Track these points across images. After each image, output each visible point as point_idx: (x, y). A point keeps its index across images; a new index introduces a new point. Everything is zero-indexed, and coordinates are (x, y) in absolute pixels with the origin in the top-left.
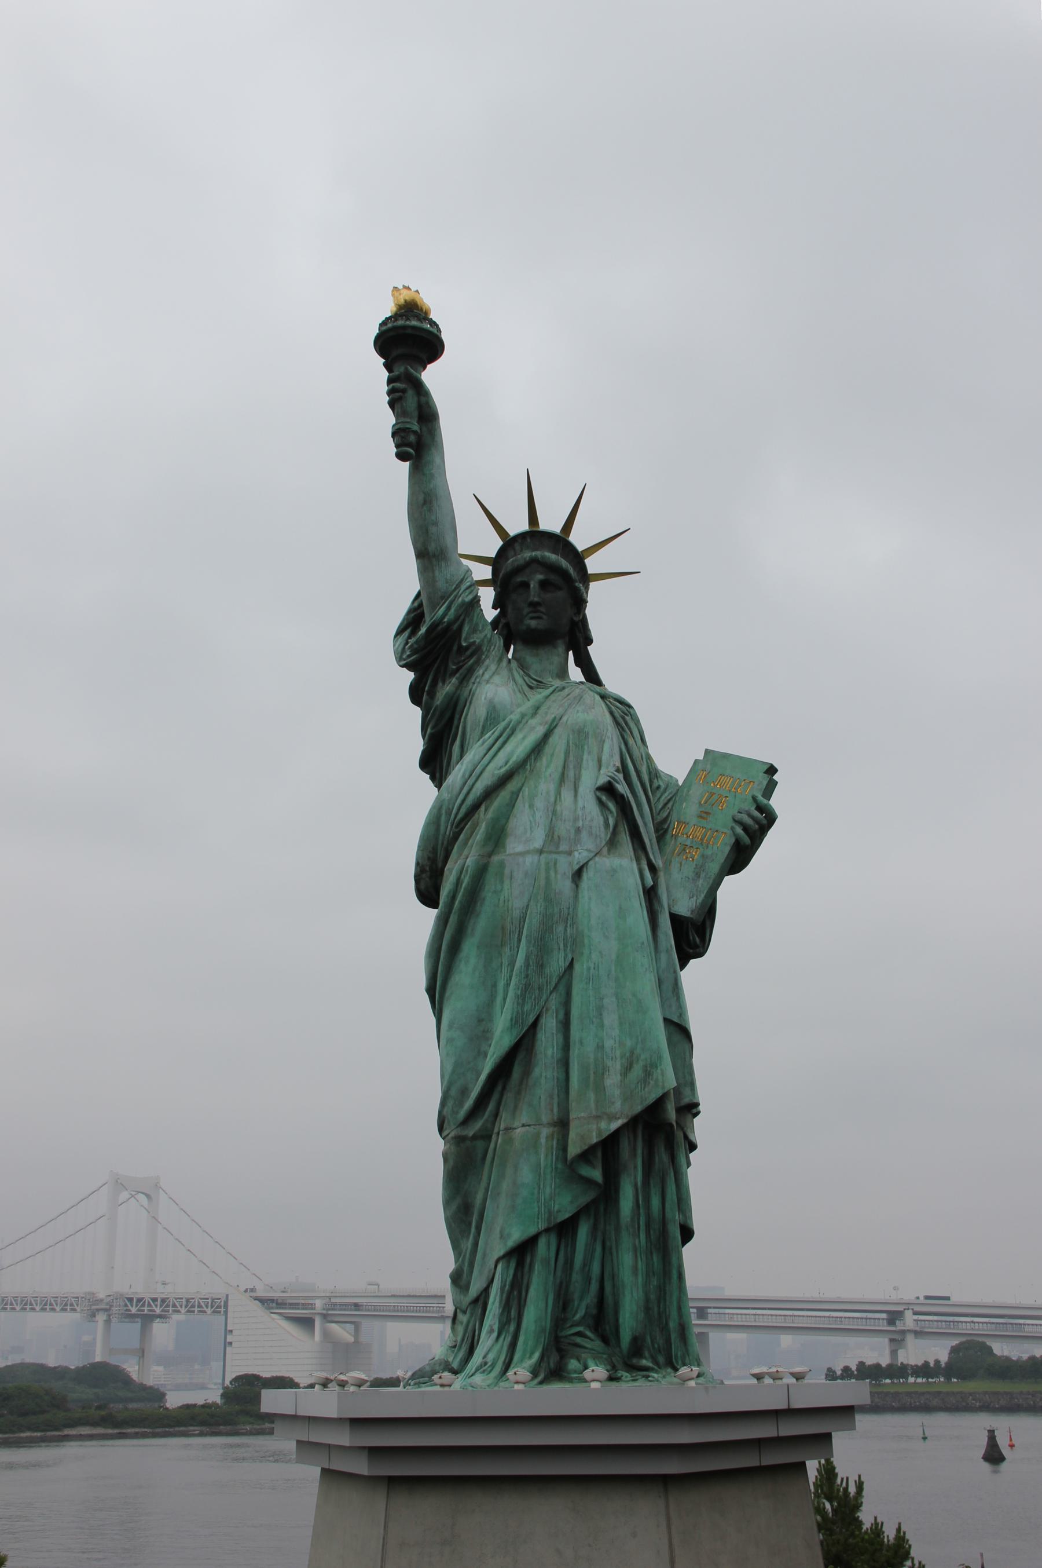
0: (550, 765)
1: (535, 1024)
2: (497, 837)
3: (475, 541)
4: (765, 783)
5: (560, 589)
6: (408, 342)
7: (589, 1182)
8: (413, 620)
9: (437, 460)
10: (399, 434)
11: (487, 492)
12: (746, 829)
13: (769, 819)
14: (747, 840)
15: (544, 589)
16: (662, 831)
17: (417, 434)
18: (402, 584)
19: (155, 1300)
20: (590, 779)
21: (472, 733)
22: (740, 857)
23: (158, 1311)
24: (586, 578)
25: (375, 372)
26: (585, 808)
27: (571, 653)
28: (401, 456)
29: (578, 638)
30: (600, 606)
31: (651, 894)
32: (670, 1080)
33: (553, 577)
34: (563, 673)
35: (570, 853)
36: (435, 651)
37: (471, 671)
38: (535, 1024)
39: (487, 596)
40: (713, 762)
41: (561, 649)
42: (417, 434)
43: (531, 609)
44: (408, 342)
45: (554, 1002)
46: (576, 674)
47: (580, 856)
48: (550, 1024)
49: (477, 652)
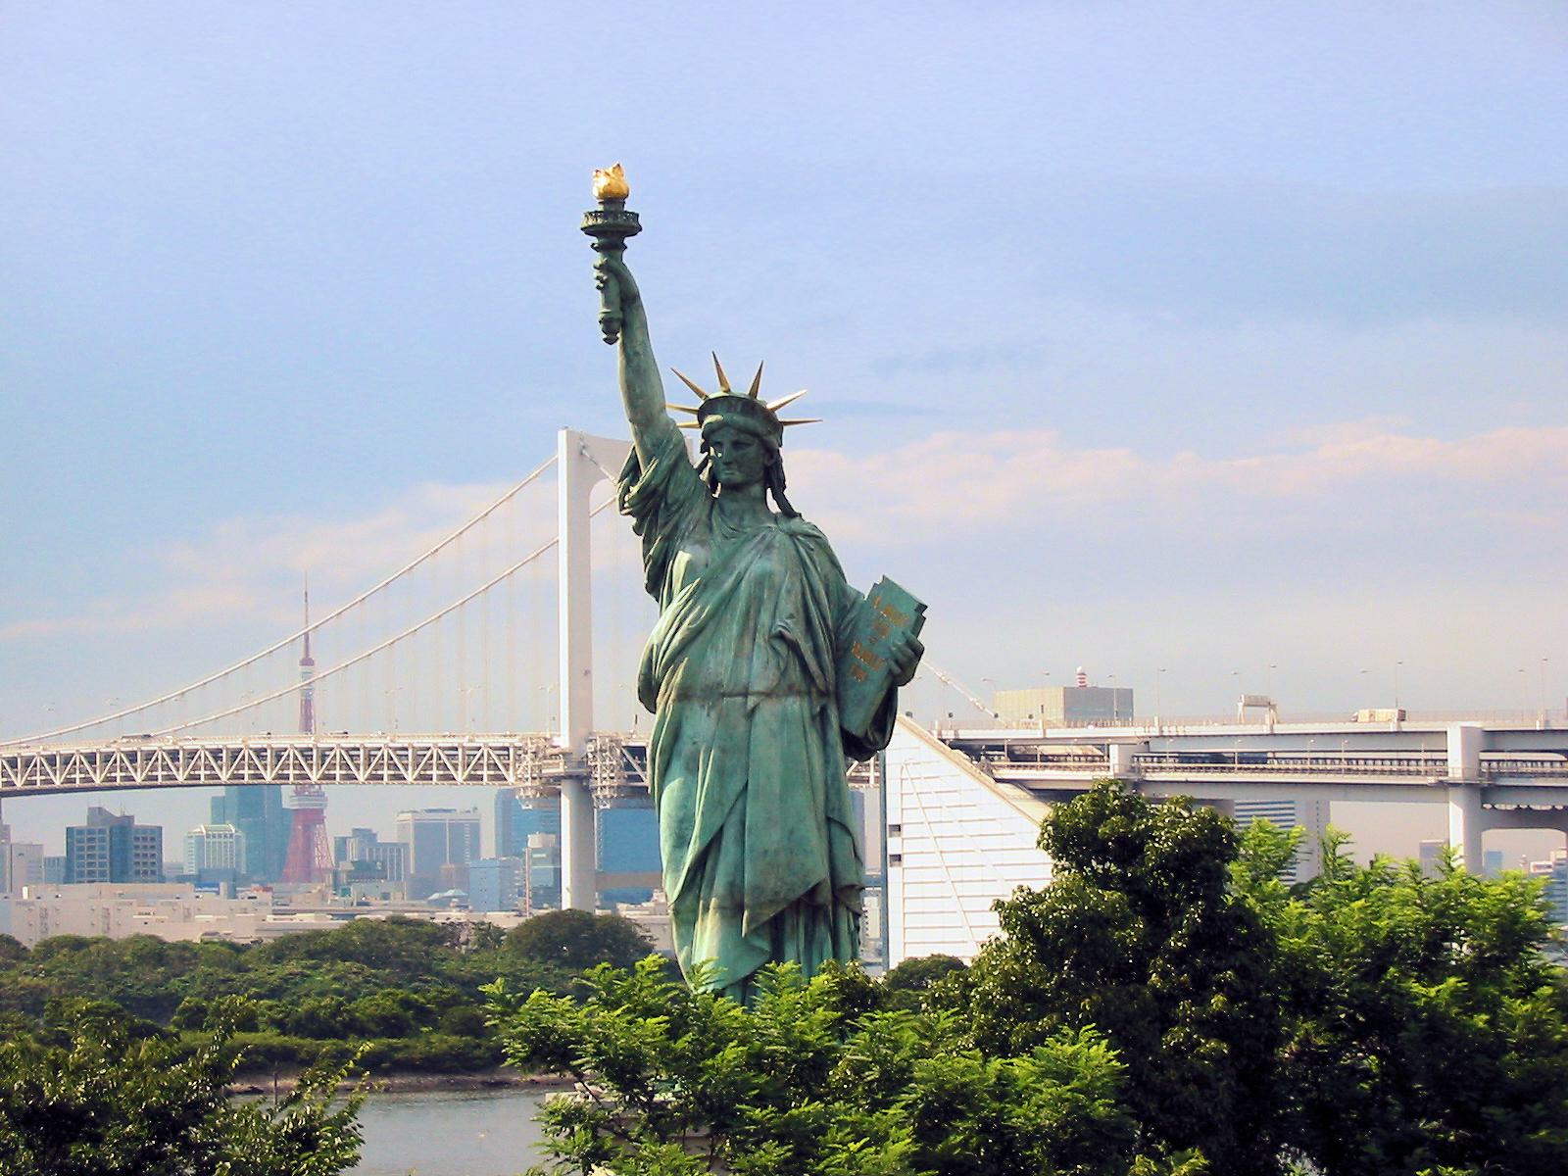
1: (721, 829)
4: (914, 618)
5: (749, 445)
6: (613, 226)
7: (762, 950)
9: (639, 337)
12: (897, 662)
13: (918, 652)
14: (897, 670)
17: (623, 312)
21: (677, 586)
24: (778, 427)
27: (769, 491)
28: (610, 341)
29: (773, 476)
32: (820, 872)
33: (743, 438)
35: (746, 694)
37: (676, 527)
38: (721, 829)
39: (694, 439)
40: (886, 588)
41: (756, 489)
42: (623, 312)
43: (725, 467)
44: (613, 226)
45: (735, 818)
46: (773, 506)
47: (751, 701)
48: (730, 834)
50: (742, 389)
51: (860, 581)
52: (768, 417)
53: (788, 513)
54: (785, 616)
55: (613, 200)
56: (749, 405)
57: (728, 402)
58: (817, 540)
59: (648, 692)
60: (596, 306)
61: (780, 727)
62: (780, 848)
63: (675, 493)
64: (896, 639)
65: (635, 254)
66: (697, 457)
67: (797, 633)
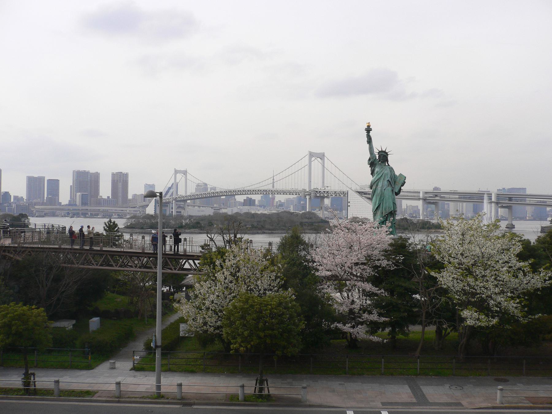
0: (382, 178)
2: (377, 185)
3: (376, 151)
6: (368, 130)
8: (370, 159)
10: (368, 142)
11: (377, 147)
15: (384, 156)
16: (395, 182)
17: (370, 141)
18: (368, 156)
19: (324, 192)
20: (387, 179)
22: (403, 185)
23: (326, 195)
25: (365, 133)
26: (386, 183)
30: (390, 158)
31: (393, 190)
34: (385, 165)
36: (372, 164)
39: (377, 156)
42: (370, 141)
44: (368, 130)
49: (376, 164)
50: (384, 150)
51: (397, 173)
52: (387, 153)
53: (388, 165)
54: (388, 178)
55: (369, 126)
56: (385, 152)
57: (382, 151)
58: (392, 168)
59: (371, 188)
60: (366, 139)
61: (388, 192)
62: (388, 206)
63: (375, 163)
64: (402, 181)
65: (371, 133)
66: (377, 158)
67: (390, 180)
